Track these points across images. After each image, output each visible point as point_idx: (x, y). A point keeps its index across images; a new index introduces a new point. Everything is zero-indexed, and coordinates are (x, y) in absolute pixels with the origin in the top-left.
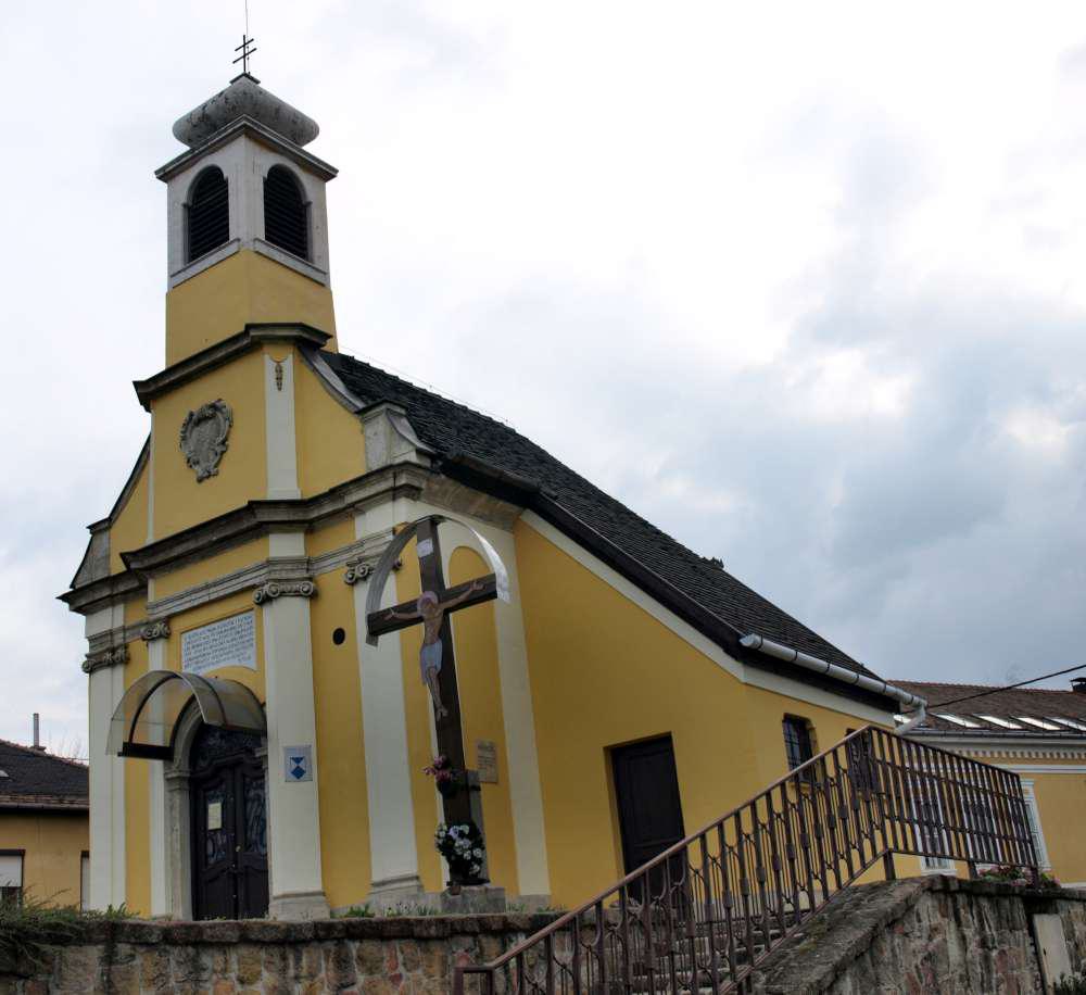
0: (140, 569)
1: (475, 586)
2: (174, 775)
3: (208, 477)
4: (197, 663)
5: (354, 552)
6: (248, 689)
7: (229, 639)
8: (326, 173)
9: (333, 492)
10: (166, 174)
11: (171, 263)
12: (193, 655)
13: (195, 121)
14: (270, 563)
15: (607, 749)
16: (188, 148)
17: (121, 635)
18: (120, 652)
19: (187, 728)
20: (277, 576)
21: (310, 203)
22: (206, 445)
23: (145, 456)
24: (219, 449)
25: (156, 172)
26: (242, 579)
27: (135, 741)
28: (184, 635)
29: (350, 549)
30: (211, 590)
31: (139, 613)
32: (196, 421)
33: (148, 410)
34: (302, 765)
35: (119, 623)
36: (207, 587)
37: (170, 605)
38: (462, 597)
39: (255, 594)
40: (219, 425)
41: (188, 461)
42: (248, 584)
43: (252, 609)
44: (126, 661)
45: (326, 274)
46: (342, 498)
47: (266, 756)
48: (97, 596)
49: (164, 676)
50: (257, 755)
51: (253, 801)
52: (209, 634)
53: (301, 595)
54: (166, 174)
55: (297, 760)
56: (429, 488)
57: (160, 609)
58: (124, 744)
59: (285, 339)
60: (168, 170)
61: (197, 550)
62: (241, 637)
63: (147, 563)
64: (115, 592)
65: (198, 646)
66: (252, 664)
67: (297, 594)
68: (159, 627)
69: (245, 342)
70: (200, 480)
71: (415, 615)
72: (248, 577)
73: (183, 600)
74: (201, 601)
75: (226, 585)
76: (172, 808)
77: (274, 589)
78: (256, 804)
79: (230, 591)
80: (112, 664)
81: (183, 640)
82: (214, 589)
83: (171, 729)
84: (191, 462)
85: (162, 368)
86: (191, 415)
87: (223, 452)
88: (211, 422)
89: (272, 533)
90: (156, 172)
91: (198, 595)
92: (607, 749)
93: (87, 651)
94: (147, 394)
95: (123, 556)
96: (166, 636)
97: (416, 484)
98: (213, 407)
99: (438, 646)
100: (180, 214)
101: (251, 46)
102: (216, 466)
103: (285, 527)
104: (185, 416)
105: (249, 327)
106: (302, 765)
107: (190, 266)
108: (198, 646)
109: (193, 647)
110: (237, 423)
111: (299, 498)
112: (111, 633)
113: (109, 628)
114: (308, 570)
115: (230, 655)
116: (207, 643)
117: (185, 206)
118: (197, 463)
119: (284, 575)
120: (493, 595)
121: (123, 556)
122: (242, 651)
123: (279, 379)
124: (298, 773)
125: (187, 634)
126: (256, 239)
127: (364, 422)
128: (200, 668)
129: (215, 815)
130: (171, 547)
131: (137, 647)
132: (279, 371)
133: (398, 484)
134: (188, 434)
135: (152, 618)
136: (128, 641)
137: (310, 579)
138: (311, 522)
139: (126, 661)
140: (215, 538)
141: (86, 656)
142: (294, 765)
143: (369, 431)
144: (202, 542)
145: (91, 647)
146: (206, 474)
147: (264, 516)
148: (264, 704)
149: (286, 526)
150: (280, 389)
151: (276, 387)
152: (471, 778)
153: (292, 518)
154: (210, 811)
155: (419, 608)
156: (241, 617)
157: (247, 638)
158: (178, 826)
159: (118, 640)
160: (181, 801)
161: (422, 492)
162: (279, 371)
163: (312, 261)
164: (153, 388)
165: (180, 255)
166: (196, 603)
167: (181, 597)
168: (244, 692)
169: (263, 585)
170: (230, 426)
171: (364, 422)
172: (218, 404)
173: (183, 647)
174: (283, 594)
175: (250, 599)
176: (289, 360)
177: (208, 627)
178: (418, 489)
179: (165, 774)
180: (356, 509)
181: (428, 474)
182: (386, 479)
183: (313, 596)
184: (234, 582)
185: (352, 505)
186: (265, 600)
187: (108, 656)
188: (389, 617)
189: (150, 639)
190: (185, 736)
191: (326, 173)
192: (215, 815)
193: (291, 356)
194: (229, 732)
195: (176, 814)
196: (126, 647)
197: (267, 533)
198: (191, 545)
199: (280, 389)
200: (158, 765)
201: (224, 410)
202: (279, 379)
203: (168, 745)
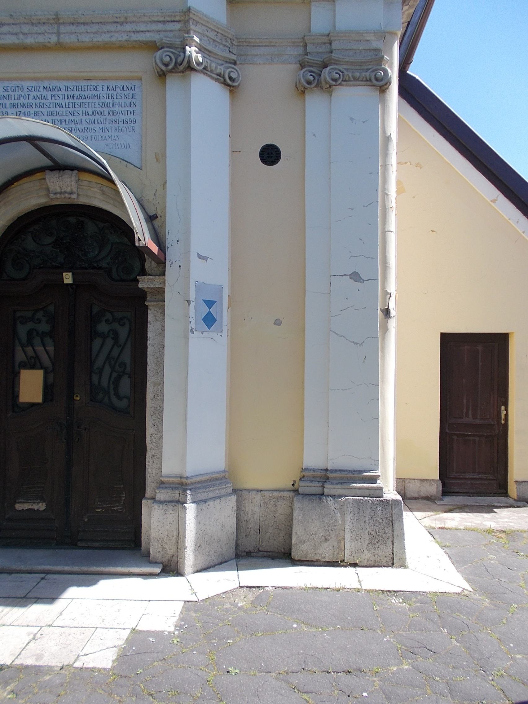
36: (57, 20)
51: (104, 336)
55: (210, 304)
65: (24, 106)
74: (41, 39)
78: (109, 342)
79: (105, 38)
82: (73, 28)
91: (36, 29)
108: (24, 106)
109: (13, 106)
115: (89, 135)
116: (42, 106)
122: (113, 134)
142: (206, 310)
157: (122, 117)
166: (30, 40)
177: (46, 84)
184: (112, 28)
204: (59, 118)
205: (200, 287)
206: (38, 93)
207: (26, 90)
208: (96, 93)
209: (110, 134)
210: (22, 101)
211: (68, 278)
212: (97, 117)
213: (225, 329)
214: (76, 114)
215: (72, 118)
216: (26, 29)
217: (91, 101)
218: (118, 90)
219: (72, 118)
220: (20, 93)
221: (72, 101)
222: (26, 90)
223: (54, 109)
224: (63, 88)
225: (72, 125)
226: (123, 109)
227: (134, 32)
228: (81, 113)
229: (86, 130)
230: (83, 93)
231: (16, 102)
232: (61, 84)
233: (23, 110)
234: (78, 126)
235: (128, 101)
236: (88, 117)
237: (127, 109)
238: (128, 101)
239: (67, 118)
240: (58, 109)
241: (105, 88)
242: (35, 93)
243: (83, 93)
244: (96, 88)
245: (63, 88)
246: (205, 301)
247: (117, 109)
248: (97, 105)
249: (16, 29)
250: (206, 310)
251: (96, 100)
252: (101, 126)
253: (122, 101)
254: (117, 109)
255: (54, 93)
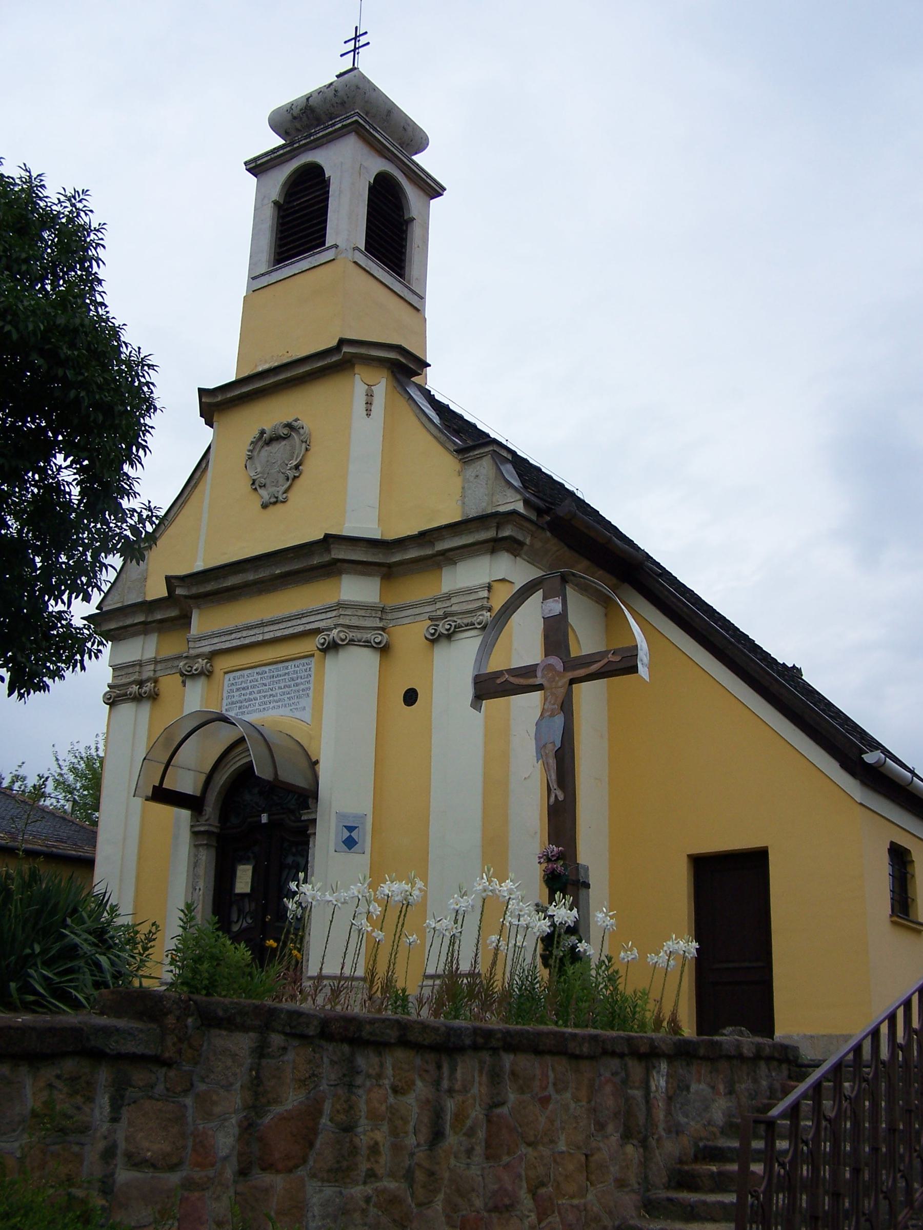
0: (186, 597)
1: (611, 657)
2: (202, 829)
3: (275, 503)
4: (240, 708)
5: (439, 605)
6: (302, 746)
7: (282, 685)
8: (433, 190)
9: (423, 534)
10: (257, 167)
11: (253, 264)
12: (236, 699)
13: (296, 112)
14: (340, 605)
15: (689, 856)
16: (282, 142)
17: (152, 667)
18: (149, 686)
19: (222, 778)
20: (346, 621)
21: (413, 219)
22: (276, 468)
23: (199, 473)
24: (291, 474)
25: (246, 163)
26: (304, 620)
27: (166, 785)
28: (226, 676)
29: (434, 601)
30: (266, 629)
31: (173, 646)
32: (267, 440)
33: (209, 423)
34: (354, 834)
35: (150, 654)
36: (262, 624)
37: (216, 640)
38: (594, 668)
39: (319, 639)
40: (293, 447)
41: (253, 484)
42: (309, 627)
43: (313, 655)
44: (154, 697)
45: (422, 298)
46: (432, 544)
47: (314, 821)
48: (129, 622)
49: (210, 717)
50: (304, 818)
52: (256, 677)
53: (372, 647)
54: (257, 167)
55: (350, 829)
56: (532, 545)
57: (204, 643)
58: (154, 786)
59: (381, 362)
60: (259, 162)
61: (255, 583)
62: (297, 685)
63: (194, 591)
64: (149, 619)
65: (244, 689)
66: (307, 716)
67: (367, 644)
68: (201, 663)
69: (334, 359)
70: (265, 506)
71: (531, 681)
72: (312, 619)
73: (233, 636)
74: (254, 639)
75: (281, 626)
76: (195, 865)
77: (342, 635)
80: (138, 699)
81: (226, 683)
83: (203, 778)
84: (255, 485)
85: (234, 379)
86: (263, 432)
87: (295, 478)
88: (284, 443)
89: (348, 573)
90: (246, 163)
92: (689, 856)
93: (110, 682)
94: (210, 405)
95: (169, 579)
96: (207, 674)
97: (520, 537)
98: (289, 426)
99: (559, 720)
100: (269, 212)
101: (363, 40)
102: (285, 492)
103: (360, 567)
104: (256, 433)
105: (342, 342)
106: (354, 834)
107: (276, 270)
108: (244, 689)
109: (238, 690)
110: (313, 449)
111: (378, 536)
112: (140, 664)
113: (139, 658)
114: (381, 619)
115: (280, 704)
116: (253, 687)
117: (276, 203)
118: (263, 486)
119: (355, 622)
120: (634, 669)
121: (169, 579)
122: (296, 700)
123: (369, 404)
124: (350, 843)
125: (232, 675)
126: (356, 249)
127: (465, 462)
128: (243, 713)
129: (244, 880)
130: (225, 577)
131: (169, 683)
132: (370, 395)
133: (500, 535)
134: (255, 453)
135: (193, 652)
136: (158, 674)
137: (383, 629)
138: (389, 566)
139: (154, 697)
140: (278, 572)
141: (109, 686)
142: (346, 834)
143: (471, 471)
144: (262, 574)
145: (114, 677)
146: (273, 500)
147: (339, 553)
148: (317, 762)
149: (362, 568)
150: (368, 415)
151: (365, 413)
152: (582, 871)
153: (371, 559)
154: (239, 873)
155: (539, 674)
156: (297, 662)
157: (302, 687)
158: (201, 885)
159: (148, 672)
160: (206, 857)
161: (525, 548)
162: (370, 395)
163: (409, 282)
164: (219, 398)
165: (265, 256)
166: (247, 641)
167: (231, 633)
168: (298, 749)
169: (330, 629)
170: (307, 450)
171: (465, 462)
172: (295, 424)
173: (226, 688)
174: (352, 643)
175: (311, 645)
176: (382, 385)
177: (258, 670)
178: (521, 544)
179: (192, 826)
180: (449, 558)
181: (533, 528)
182: (487, 529)
183: (384, 650)
185: (443, 553)
186: (332, 647)
187: (135, 688)
188: (499, 681)
189: (188, 676)
190: (217, 789)
191: (433, 190)
192: (244, 880)
193: (384, 382)
194: (289, 789)
195: (201, 871)
196: (156, 681)
197: (339, 573)
198: (251, 577)
199: (368, 415)
200: (185, 814)
201: (301, 431)
202: (369, 404)
203: (198, 794)
204: (264, 694)
205: (341, 816)
206: (252, 678)
207: (246, 676)
208: (287, 671)
209: (293, 701)
210: (244, 685)
211: (264, 818)
212: (287, 689)
213: (368, 850)
214: (274, 689)
215: (271, 693)
216: (244, 634)
217: (283, 678)
218: (301, 667)
219: (271, 693)
220: (243, 679)
221: (272, 680)
222: (246, 676)
223: (262, 688)
224: (267, 671)
225: (271, 698)
226: (303, 681)
227: (307, 623)
228: (277, 688)
229: (280, 700)
230: (279, 673)
231: (239, 686)
232: (266, 669)
233: (243, 692)
234: (275, 698)
235: (306, 674)
236: (281, 691)
237: (305, 680)
238: (306, 674)
239: (268, 694)
240: (264, 688)
241: (293, 666)
242: (251, 678)
243: (279, 673)
244: (287, 668)
245: (267, 671)
246: (345, 826)
247: (299, 681)
248: (287, 680)
249: (239, 635)
250: (346, 834)
251: (286, 677)
252: (288, 696)
253: (302, 674)
254: (299, 681)
255: (262, 676)
